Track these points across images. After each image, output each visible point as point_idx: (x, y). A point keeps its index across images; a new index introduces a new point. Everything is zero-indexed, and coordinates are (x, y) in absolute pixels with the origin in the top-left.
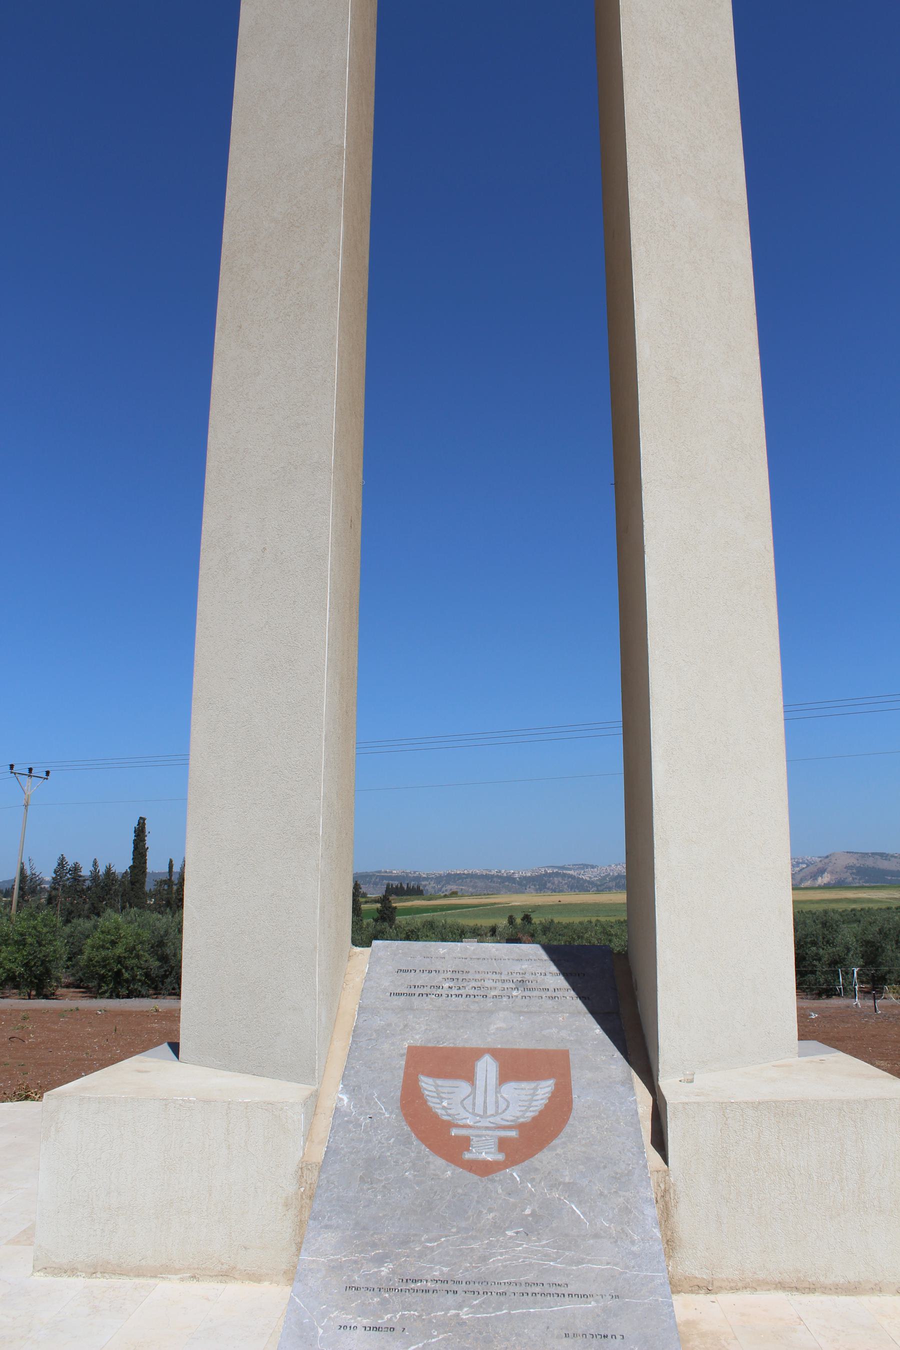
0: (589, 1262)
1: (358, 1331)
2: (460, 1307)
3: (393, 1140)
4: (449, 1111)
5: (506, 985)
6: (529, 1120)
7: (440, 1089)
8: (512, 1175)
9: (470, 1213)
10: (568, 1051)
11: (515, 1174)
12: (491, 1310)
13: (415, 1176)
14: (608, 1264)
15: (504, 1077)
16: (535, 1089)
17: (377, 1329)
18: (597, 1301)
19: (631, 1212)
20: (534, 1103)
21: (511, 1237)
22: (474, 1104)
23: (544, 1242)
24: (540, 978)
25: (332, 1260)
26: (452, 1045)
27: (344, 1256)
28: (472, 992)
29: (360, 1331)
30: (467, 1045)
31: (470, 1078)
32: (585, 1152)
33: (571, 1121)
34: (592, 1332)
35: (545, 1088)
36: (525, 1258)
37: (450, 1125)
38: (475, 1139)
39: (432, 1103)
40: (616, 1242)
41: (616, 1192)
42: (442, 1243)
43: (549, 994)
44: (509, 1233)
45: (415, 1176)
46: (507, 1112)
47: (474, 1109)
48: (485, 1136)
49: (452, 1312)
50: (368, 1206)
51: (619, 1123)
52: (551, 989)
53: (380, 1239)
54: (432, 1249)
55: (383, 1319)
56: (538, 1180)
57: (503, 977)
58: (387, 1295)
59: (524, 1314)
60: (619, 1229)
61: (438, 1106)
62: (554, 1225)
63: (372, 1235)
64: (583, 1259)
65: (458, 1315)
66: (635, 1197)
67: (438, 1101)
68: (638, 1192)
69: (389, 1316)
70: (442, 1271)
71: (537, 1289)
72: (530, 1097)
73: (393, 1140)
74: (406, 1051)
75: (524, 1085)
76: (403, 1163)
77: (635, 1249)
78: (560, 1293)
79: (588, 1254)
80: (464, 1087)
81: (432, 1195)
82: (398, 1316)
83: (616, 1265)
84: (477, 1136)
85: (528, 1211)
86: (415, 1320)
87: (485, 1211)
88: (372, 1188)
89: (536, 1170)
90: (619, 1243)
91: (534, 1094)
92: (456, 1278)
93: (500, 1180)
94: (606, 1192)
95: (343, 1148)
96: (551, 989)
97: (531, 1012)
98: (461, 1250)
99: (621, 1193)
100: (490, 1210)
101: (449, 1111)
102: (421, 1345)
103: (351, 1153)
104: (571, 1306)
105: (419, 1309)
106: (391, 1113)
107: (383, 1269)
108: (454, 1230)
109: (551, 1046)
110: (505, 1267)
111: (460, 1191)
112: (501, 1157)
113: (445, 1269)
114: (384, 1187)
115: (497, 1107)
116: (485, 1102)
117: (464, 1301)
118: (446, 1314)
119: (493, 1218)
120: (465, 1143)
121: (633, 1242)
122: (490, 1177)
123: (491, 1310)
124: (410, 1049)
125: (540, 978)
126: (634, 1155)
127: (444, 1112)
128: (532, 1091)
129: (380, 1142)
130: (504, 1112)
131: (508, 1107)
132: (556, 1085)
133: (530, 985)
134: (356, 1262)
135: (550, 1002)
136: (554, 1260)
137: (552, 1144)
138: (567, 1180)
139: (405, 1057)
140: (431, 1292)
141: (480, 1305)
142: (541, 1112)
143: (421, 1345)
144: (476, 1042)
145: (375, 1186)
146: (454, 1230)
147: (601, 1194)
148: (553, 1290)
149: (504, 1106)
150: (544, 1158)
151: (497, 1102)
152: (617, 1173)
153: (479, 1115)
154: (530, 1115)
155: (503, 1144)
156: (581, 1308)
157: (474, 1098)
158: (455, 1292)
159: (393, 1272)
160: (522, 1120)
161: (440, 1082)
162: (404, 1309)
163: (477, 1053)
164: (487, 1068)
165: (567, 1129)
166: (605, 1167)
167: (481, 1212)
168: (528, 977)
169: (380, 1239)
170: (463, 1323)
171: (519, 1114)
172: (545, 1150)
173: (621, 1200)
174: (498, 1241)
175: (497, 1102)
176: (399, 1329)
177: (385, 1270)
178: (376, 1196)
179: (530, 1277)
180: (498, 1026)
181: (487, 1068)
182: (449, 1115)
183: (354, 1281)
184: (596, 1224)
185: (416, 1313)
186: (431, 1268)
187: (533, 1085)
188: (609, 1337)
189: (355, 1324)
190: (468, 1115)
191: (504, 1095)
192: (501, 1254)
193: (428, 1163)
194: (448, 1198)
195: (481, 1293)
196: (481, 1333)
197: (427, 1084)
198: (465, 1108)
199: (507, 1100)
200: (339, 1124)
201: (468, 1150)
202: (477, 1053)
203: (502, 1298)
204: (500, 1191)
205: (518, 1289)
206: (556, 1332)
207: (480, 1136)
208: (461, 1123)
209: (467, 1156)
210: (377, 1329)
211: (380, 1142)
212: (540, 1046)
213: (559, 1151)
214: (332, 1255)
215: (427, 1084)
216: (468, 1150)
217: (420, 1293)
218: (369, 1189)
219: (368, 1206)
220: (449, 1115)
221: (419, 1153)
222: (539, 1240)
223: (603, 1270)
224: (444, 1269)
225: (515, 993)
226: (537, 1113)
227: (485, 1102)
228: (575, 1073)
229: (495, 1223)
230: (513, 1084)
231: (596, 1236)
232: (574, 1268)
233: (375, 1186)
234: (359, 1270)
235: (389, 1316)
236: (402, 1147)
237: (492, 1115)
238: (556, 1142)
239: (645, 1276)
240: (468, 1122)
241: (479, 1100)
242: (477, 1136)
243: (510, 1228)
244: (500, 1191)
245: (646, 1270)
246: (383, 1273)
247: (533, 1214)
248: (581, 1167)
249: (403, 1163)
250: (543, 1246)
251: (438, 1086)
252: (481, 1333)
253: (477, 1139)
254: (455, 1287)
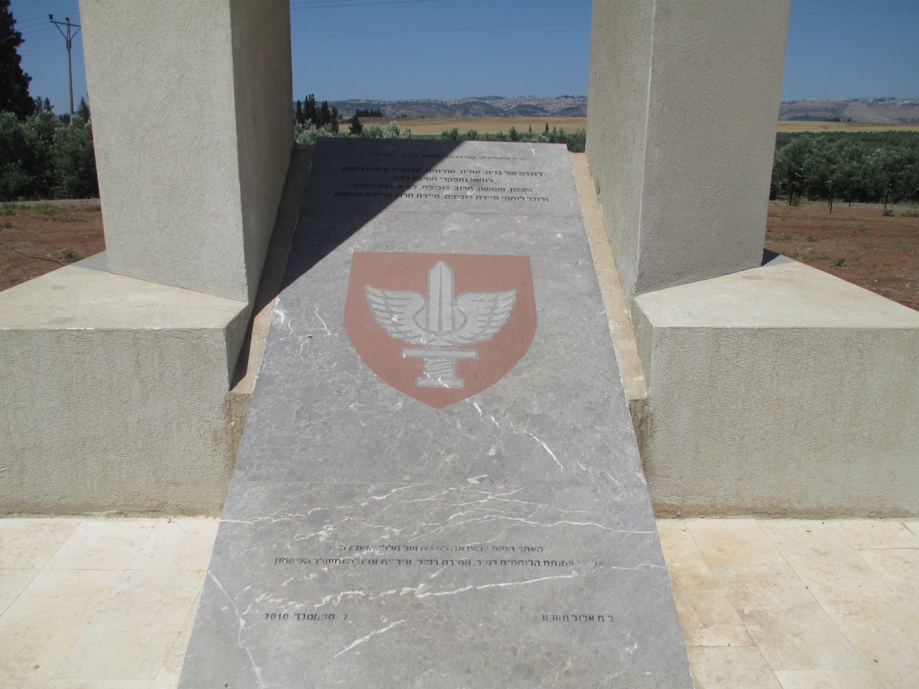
0: (567, 517)
1: (289, 621)
2: (415, 584)
3: (335, 364)
4: (400, 328)
5: (459, 185)
6: (489, 337)
7: (389, 301)
8: (472, 405)
9: (425, 455)
10: (528, 257)
11: (476, 405)
12: (452, 585)
13: (361, 409)
14: (588, 519)
15: (460, 288)
16: (495, 301)
17: (313, 617)
18: (578, 570)
19: (610, 452)
20: (495, 318)
21: (474, 486)
22: (427, 319)
23: (513, 492)
24: (495, 178)
25: (260, 523)
26: (401, 250)
27: (275, 517)
28: (423, 192)
29: (292, 622)
30: (420, 251)
31: (423, 288)
32: (553, 377)
33: (536, 339)
34: (575, 612)
35: (505, 301)
36: (491, 513)
37: (401, 344)
38: (430, 361)
39: (380, 317)
40: (596, 490)
41: (591, 426)
42: (392, 496)
43: (506, 194)
44: (473, 481)
45: (361, 409)
46: (465, 327)
47: (427, 325)
48: (440, 357)
49: (406, 590)
50: (305, 448)
51: (590, 342)
52: (508, 189)
53: (318, 493)
54: (380, 504)
55: (320, 602)
56: (503, 412)
57: (456, 176)
58: (326, 569)
59: (492, 591)
60: (598, 473)
61: (387, 322)
62: (523, 469)
63: (309, 488)
64: (559, 513)
65: (412, 594)
66: (613, 432)
67: (388, 316)
68: (616, 427)
69: (328, 598)
70: (392, 533)
71: (507, 556)
72: (489, 310)
73: (335, 364)
74: (351, 258)
75: (483, 296)
76: (348, 392)
77: (618, 499)
78: (534, 560)
79: (565, 507)
80: (417, 300)
81: (381, 433)
82: (339, 598)
83: (598, 521)
84: (430, 358)
85: (492, 452)
86: (360, 603)
87: (443, 453)
88: (310, 425)
89: (500, 398)
90: (599, 491)
91: (494, 308)
92: (410, 543)
93: (459, 412)
94: (580, 427)
95: (277, 376)
96: (508, 189)
97: (487, 214)
98: (414, 505)
99: (597, 427)
100: (449, 451)
101: (400, 328)
102: (367, 637)
103: (287, 381)
104: (546, 577)
105: (365, 587)
106: (333, 332)
107: (321, 533)
108: (407, 478)
109: (510, 252)
110: (468, 525)
111: (413, 426)
112: (459, 384)
113: (397, 531)
114: (325, 423)
115: (454, 323)
116: (440, 317)
117: (419, 574)
118: (398, 593)
119: (452, 461)
120: (417, 367)
121: (615, 490)
122: (447, 408)
123: (452, 585)
124: (356, 254)
125: (495, 178)
126: (609, 380)
127: (393, 329)
128: (492, 304)
129: (321, 367)
130: (461, 328)
131: (465, 322)
132: (517, 296)
133: (485, 185)
134: (288, 524)
135: (507, 203)
136: (526, 516)
137: (516, 367)
138: (535, 411)
139: (350, 265)
140: (379, 563)
141: (438, 580)
142: (503, 329)
143: (367, 637)
144: (429, 247)
145: (314, 423)
146: (407, 478)
147: (575, 429)
148: (525, 556)
149: (461, 321)
150: (508, 386)
151: (453, 317)
152: (590, 403)
153: (433, 332)
154: (491, 331)
155: (462, 368)
156: (560, 579)
157: (428, 312)
158: (409, 562)
159: (334, 536)
160: (482, 338)
161: (389, 293)
162: (347, 587)
163: (431, 260)
164: (441, 278)
165: (533, 349)
166: (577, 395)
167: (437, 453)
168: (482, 176)
169: (318, 493)
170: (419, 605)
171: (478, 331)
172: (509, 374)
173: (598, 436)
174: (458, 491)
175: (453, 317)
176: (340, 616)
177: (324, 534)
178: (314, 436)
179: (499, 539)
180: (452, 228)
181: (441, 278)
182: (400, 333)
183: (286, 550)
184: (571, 467)
185: (361, 593)
186: (379, 529)
187: (492, 296)
188: (596, 619)
189: (286, 611)
190: (421, 332)
191: (462, 309)
192: (463, 509)
193: (376, 392)
194: (399, 436)
195: (440, 562)
196: (440, 618)
197: (376, 297)
198: (417, 324)
199: (463, 314)
200: (274, 347)
201: (421, 375)
202: (431, 260)
203: (466, 569)
204: (459, 426)
205: (482, 556)
206: (531, 614)
207: (436, 358)
208: (413, 342)
209: (421, 383)
210: (313, 617)
211: (321, 367)
212: (498, 253)
213: (525, 375)
214: (261, 515)
215: (376, 297)
216: (421, 375)
217: (366, 565)
218: (306, 427)
219: (305, 448)
220: (400, 333)
221: (365, 379)
222: (507, 489)
223: (583, 527)
224: (395, 530)
225: (469, 193)
226: (498, 330)
227: (440, 317)
228: (537, 283)
229: (455, 467)
230: (471, 296)
231: (573, 483)
232: (549, 525)
233: (314, 423)
234: (292, 535)
235: (328, 598)
236: (346, 373)
237: (448, 332)
238: (521, 364)
239: (632, 535)
240: (422, 341)
241: (433, 315)
242: (430, 358)
243: (472, 474)
244: (459, 426)
245: (633, 527)
246: (321, 539)
247: (499, 455)
248: (550, 395)
249: (348, 392)
250: (512, 497)
251: (387, 298)
252: (440, 618)
253: (432, 361)
254: (409, 555)
